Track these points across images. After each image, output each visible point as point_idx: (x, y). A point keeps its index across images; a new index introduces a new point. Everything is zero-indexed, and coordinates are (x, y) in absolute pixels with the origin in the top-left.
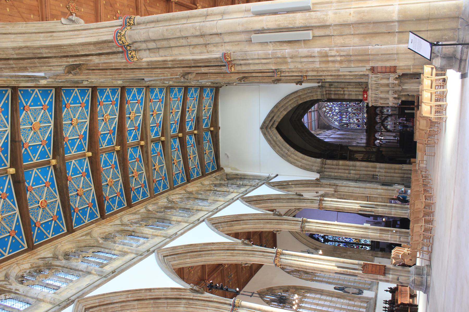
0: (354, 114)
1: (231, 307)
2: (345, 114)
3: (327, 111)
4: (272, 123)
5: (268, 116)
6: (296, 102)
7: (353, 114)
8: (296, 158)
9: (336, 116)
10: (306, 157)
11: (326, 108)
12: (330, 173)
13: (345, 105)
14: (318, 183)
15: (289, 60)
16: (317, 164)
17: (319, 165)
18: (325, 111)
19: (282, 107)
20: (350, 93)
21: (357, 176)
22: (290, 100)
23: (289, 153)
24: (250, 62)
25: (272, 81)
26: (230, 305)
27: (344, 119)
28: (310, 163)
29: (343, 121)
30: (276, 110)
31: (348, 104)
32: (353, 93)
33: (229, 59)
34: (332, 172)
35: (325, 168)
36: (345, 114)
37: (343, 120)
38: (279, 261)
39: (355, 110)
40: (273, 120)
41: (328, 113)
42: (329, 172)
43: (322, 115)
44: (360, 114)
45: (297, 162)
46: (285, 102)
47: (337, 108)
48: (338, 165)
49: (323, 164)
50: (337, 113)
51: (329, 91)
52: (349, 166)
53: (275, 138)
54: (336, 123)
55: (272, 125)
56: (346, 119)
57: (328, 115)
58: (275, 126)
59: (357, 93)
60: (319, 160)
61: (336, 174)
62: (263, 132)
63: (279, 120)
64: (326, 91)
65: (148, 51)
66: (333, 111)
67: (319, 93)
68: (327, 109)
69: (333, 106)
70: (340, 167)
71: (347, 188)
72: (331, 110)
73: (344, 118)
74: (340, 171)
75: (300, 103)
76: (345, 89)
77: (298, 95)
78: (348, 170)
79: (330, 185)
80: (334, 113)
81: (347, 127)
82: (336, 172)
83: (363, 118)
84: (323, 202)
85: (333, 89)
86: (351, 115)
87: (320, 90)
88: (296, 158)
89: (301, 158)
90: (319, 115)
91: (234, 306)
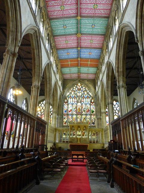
0: (76, 107)
2: (76, 100)
3: (78, 86)
7: (76, 107)
11: (80, 85)
18: (78, 85)
27: (71, 99)
31: (84, 102)
37: (70, 99)
39: (79, 108)
41: (76, 87)
47: (80, 94)
50: (76, 94)
54: (68, 94)
56: (71, 101)
66: (78, 91)
68: (79, 87)
69: (82, 91)
72: (79, 90)
73: (73, 99)
80: (76, 92)
81: (66, 103)
86: (75, 105)
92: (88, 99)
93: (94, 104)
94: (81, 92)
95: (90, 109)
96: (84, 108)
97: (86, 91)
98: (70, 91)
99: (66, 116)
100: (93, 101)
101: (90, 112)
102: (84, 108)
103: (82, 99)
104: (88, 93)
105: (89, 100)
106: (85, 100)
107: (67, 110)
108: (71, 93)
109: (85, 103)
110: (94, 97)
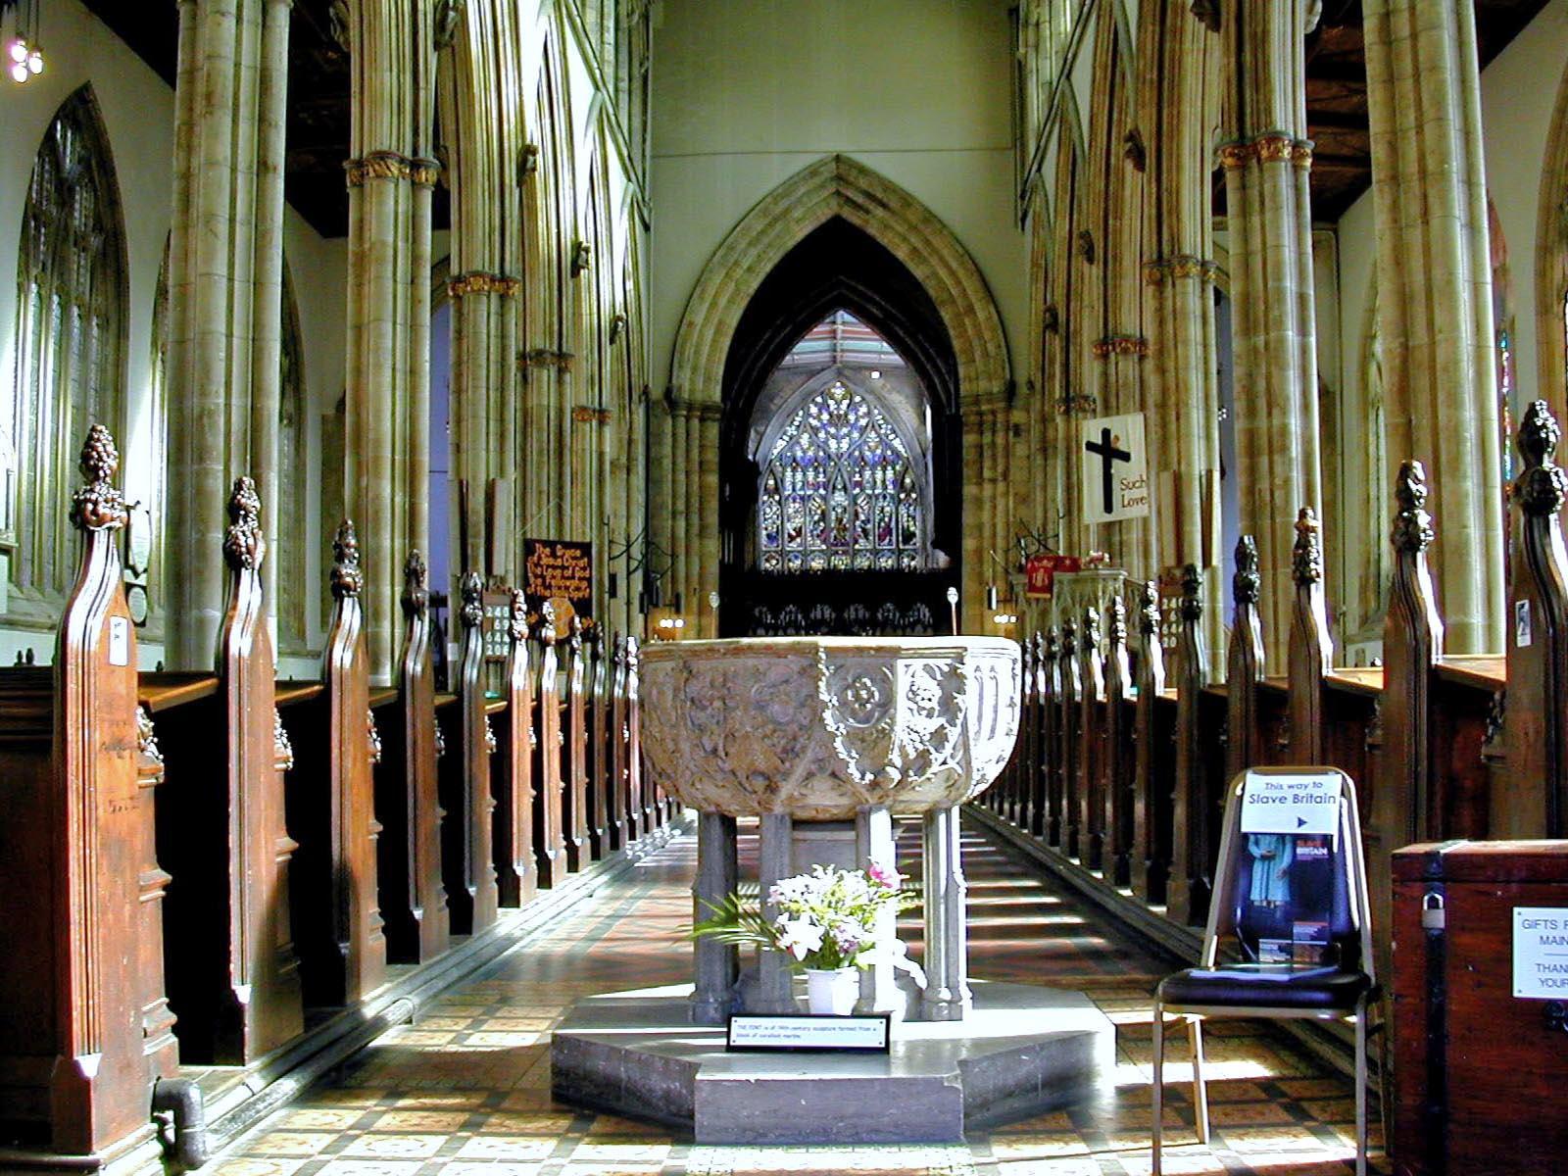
0: (824, 516)
1: (408, 153)
2: (821, 478)
3: (831, 402)
4: (860, 199)
5: (888, 186)
6: (945, 296)
7: (823, 512)
8: (723, 301)
9: (811, 444)
10: (726, 343)
12: (669, 440)
13: (857, 478)
14: (635, 397)
15: (1260, 340)
16: (700, 385)
17: (699, 397)
19: (928, 243)
20: (987, 506)
21: (665, 543)
22: (952, 273)
23: (739, 273)
24: (1256, 220)
25: (1087, 232)
26: (415, 151)
27: (799, 476)
28: (703, 360)
29: (789, 473)
30: (912, 216)
32: (986, 516)
33: (1264, 153)
34: (674, 447)
35: (688, 419)
36: (821, 478)
37: (794, 470)
38: (479, 292)
39: (840, 521)
40: (871, 206)
42: (674, 435)
43: (812, 383)
44: (824, 542)
45: (707, 305)
46: (945, 252)
47: (845, 444)
48: (702, 470)
49: (706, 408)
51: (994, 423)
52: (701, 510)
53: (797, 214)
54: (781, 444)
55: (848, 200)
57: (814, 410)
58: (848, 214)
59: (987, 533)
60: (716, 394)
61: (667, 463)
62: (823, 163)
63: (873, 230)
64: (993, 413)
65: (1383, 11)
66: (833, 430)
67: (983, 385)
68: (838, 403)
70: (695, 478)
71: (624, 507)
72: (838, 420)
74: (682, 477)
75: (943, 314)
76: (1001, 486)
77: (977, 306)
78: (688, 507)
79: (630, 442)
80: (822, 435)
82: (674, 463)
83: (805, 554)
84: (594, 423)
85: (1000, 440)
87: (995, 390)
88: (723, 301)
89: (721, 323)
90: (811, 372)
91: (416, 165)
92: (884, 470)
93: (914, 496)
94: (848, 435)
95: (893, 524)
96: (862, 517)
97: (873, 426)
98: (792, 431)
99: (774, 562)
100: (908, 481)
101: (894, 538)
102: (862, 517)
103: (851, 475)
104: (883, 442)
105: (890, 474)
106: (867, 474)
107: (780, 530)
108: (794, 441)
109: (870, 492)
110: (916, 465)
